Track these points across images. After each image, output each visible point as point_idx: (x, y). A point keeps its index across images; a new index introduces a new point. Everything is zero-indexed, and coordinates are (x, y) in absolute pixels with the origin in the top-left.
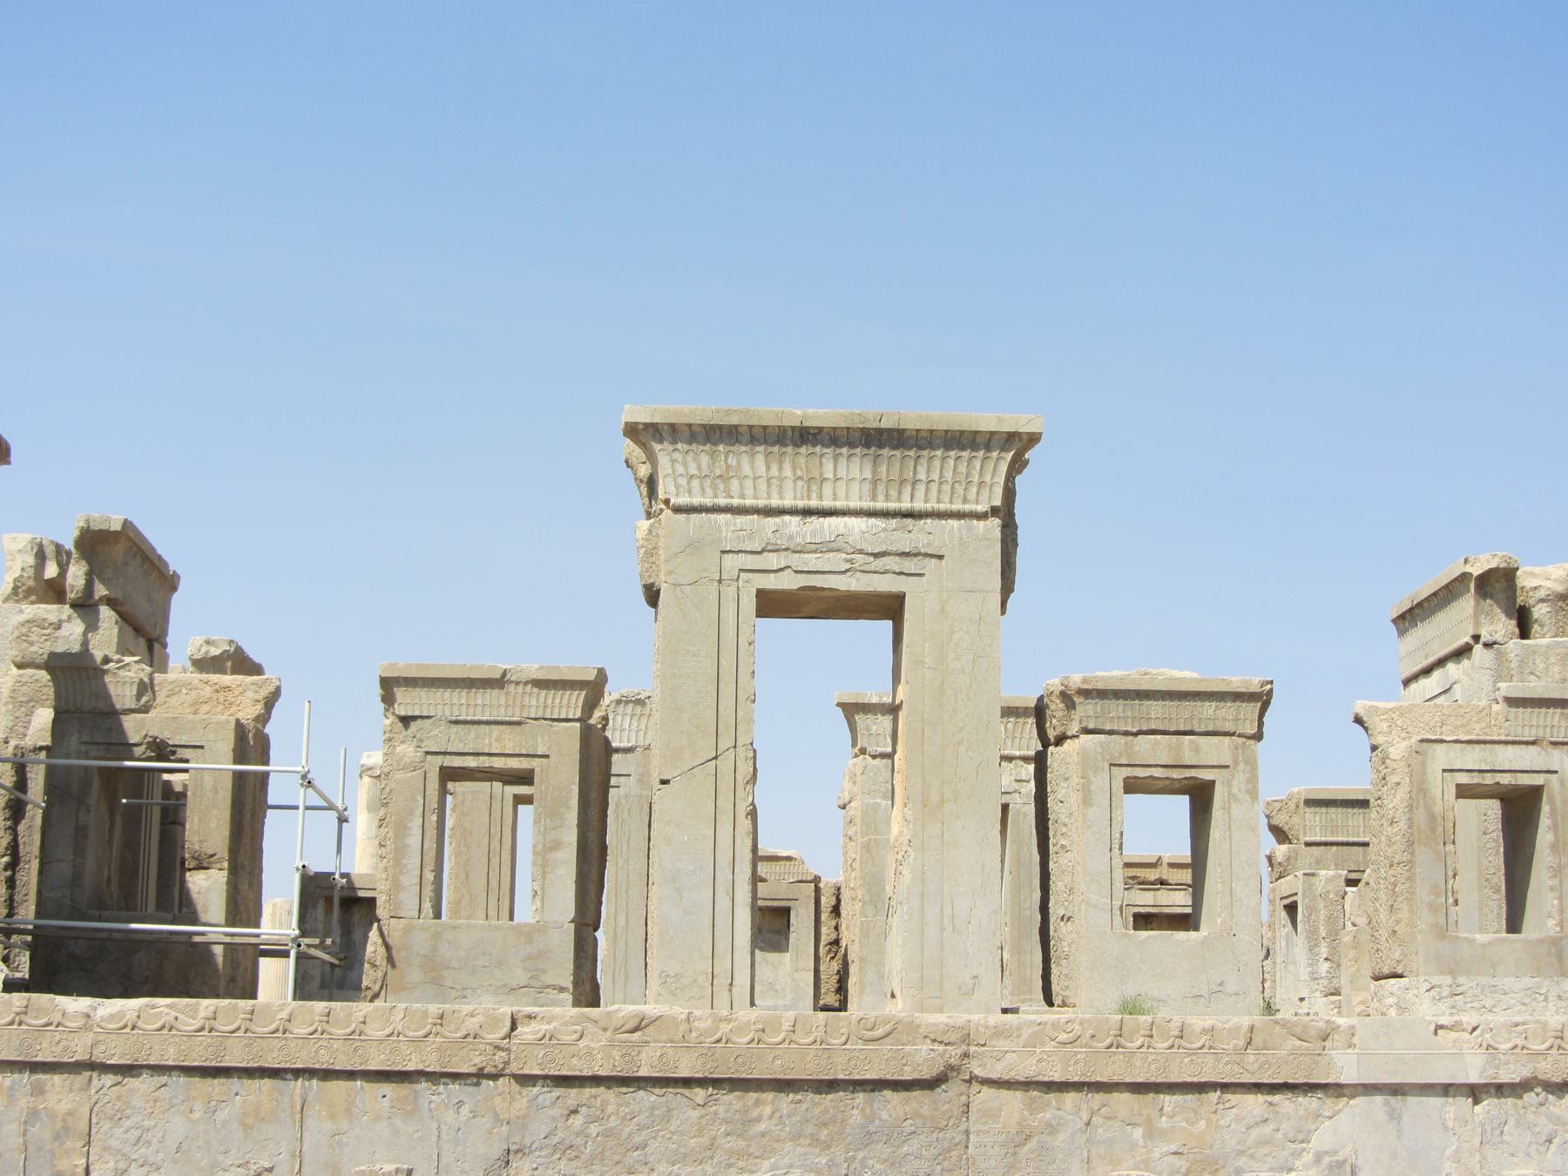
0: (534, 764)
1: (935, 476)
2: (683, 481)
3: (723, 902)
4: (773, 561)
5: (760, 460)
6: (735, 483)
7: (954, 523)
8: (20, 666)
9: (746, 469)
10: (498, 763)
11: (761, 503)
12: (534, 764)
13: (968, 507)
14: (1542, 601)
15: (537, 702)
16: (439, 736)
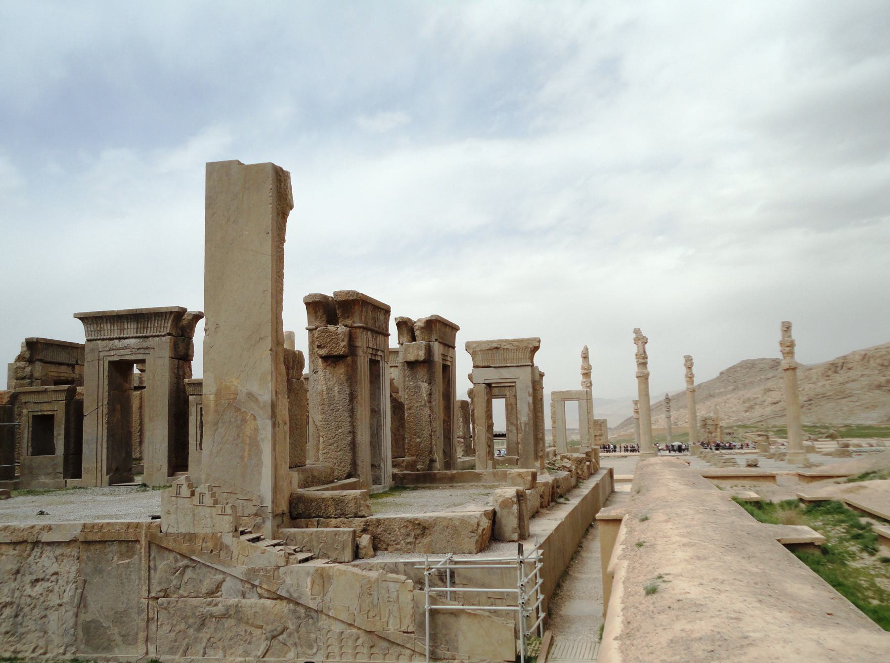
0: (55, 413)
1: (153, 326)
2: (90, 332)
3: (99, 448)
4: (112, 353)
5: (109, 325)
6: (103, 332)
7: (157, 339)
8: (17, 379)
9: (105, 328)
10: (46, 413)
11: (108, 337)
12: (55, 413)
13: (160, 334)
14: (417, 330)
15: (54, 397)
16: (32, 407)
